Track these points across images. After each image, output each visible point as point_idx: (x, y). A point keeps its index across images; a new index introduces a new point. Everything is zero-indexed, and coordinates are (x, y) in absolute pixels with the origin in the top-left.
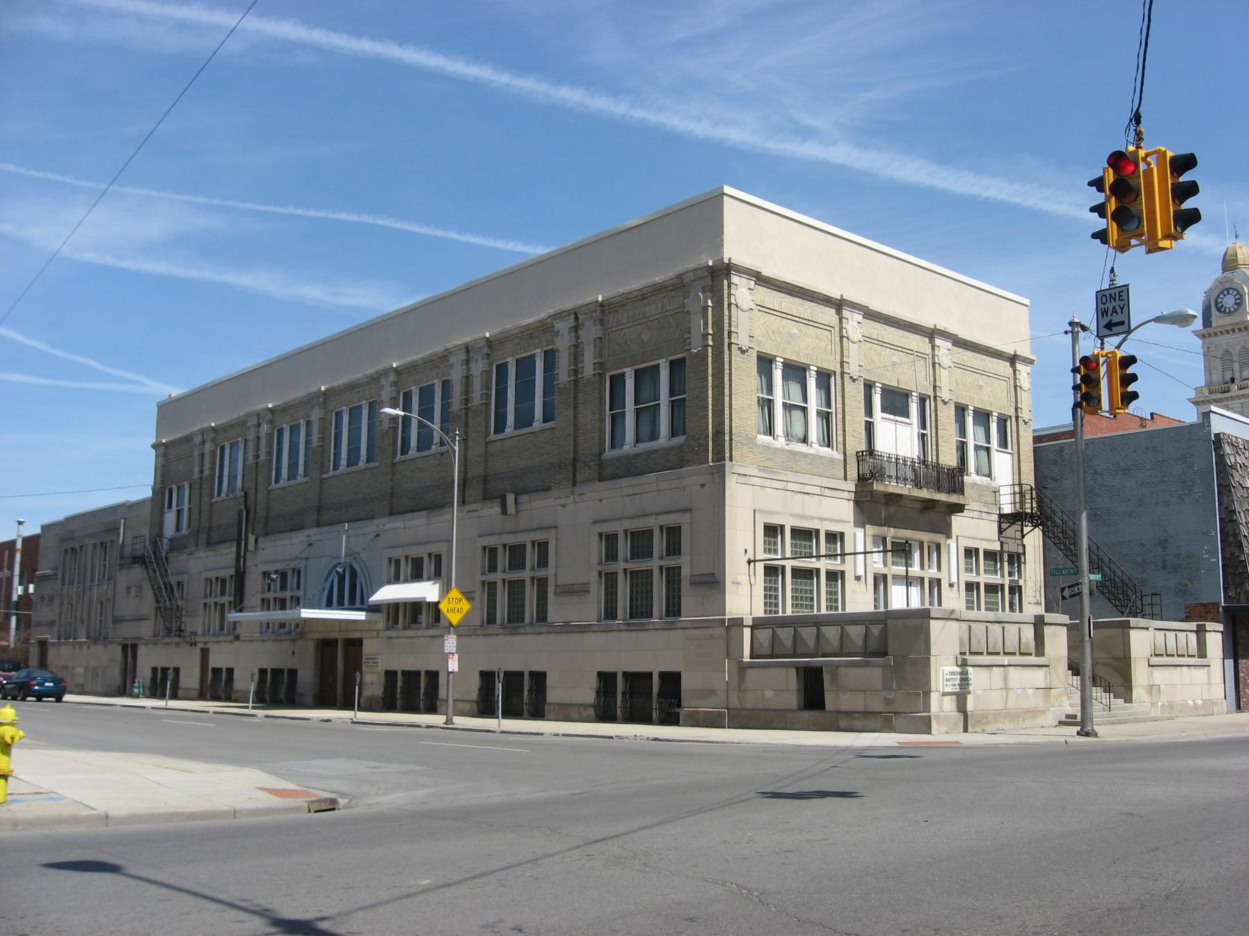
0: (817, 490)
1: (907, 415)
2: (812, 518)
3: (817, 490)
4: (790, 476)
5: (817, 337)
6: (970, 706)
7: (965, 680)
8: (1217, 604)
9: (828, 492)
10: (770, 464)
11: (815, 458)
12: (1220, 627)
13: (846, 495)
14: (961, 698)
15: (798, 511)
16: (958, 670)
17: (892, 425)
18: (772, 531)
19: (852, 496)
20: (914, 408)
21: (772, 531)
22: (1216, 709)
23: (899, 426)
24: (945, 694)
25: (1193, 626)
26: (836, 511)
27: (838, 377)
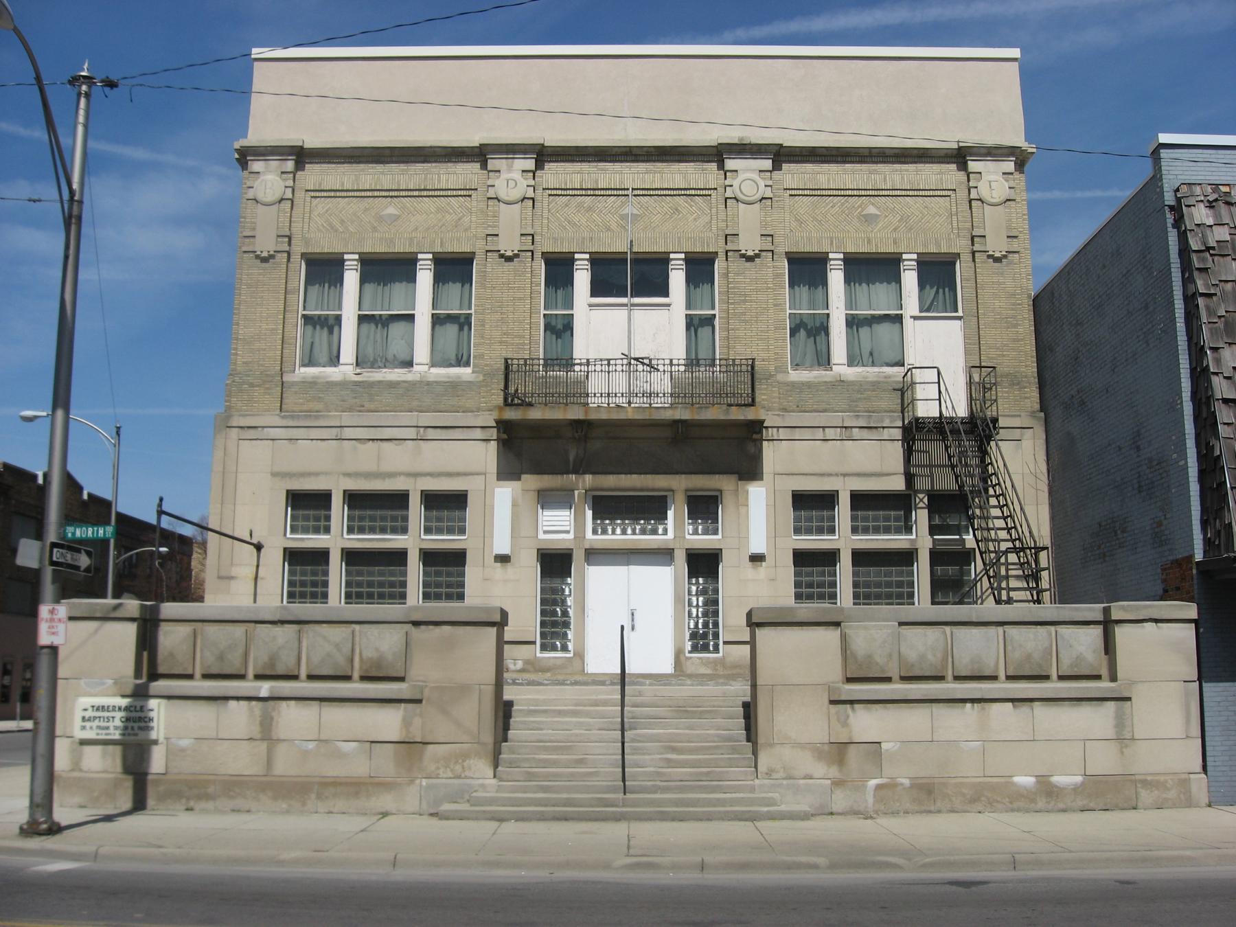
0: (411, 433)
1: (665, 292)
2: (392, 475)
3: (411, 433)
4: (347, 418)
5: (439, 210)
6: (158, 762)
7: (137, 720)
8: (1192, 556)
9: (431, 434)
10: (312, 405)
11: (426, 385)
12: (1191, 611)
13: (478, 434)
14: (134, 749)
15: (371, 467)
16: (124, 702)
17: (623, 313)
18: (307, 504)
19: (493, 433)
20: (677, 279)
21: (307, 504)
22: (1146, 796)
23: (638, 314)
24: (83, 742)
25: (1093, 611)
26: (471, 459)
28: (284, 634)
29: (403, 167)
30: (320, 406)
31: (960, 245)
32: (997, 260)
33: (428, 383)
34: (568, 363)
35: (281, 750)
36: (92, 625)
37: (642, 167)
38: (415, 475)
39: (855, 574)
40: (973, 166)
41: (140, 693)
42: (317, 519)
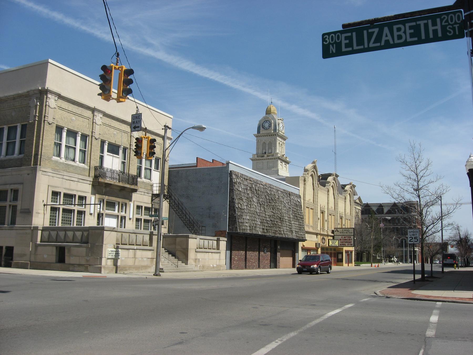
0: (76, 180)
1: (118, 154)
2: (73, 190)
3: (76, 180)
4: (65, 173)
5: (83, 121)
6: (119, 263)
7: (117, 254)
8: (226, 231)
9: (81, 181)
10: (56, 168)
11: (77, 167)
12: (226, 239)
13: (89, 182)
14: (115, 261)
15: (68, 187)
16: (115, 250)
17: (112, 157)
18: (55, 194)
19: (91, 183)
20: (121, 152)
21: (55, 194)
22: (221, 268)
23: (114, 158)
24: (108, 259)
25: (216, 238)
26: (84, 188)
27: (90, 137)
28: (133, 236)
29: (77, 107)
30: (58, 168)
31: (128, 146)
32: (50, 124)
33: (80, 167)
34: (103, 169)
35: (137, 259)
36: (109, 232)
37: (119, 123)
38: (77, 191)
39: (51, 213)
40: (96, 113)
41: (117, 248)
42: (70, 201)
